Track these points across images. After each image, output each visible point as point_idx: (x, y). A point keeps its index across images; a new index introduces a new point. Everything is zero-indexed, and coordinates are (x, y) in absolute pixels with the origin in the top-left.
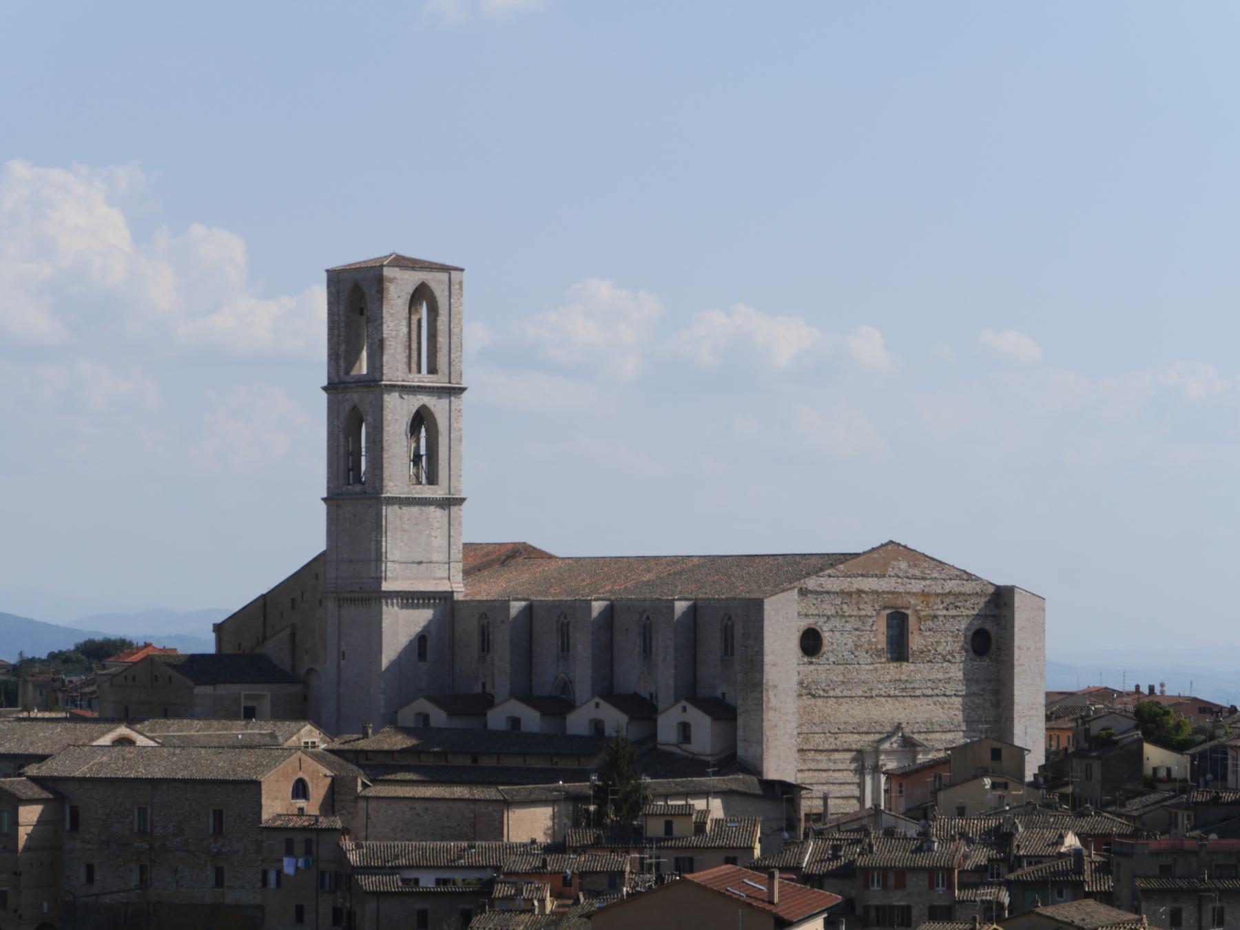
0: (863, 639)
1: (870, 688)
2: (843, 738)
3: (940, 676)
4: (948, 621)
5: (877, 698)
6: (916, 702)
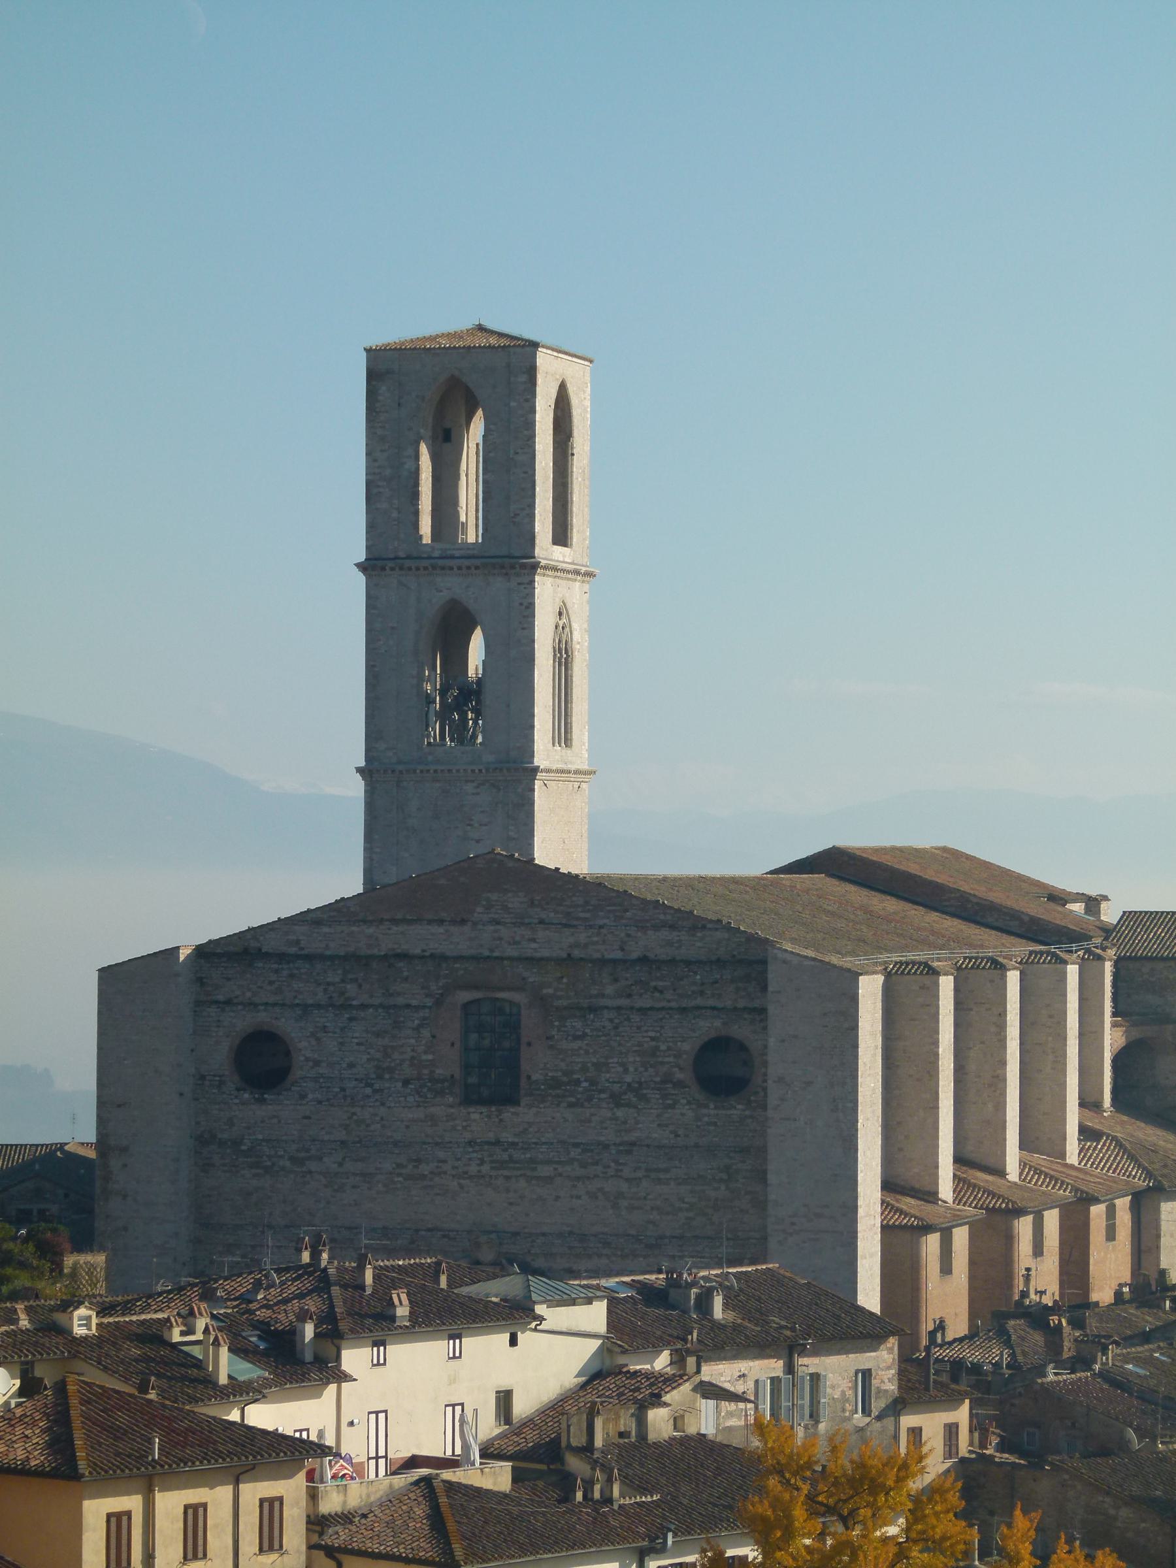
0: (396, 1056)
5: (437, 1179)
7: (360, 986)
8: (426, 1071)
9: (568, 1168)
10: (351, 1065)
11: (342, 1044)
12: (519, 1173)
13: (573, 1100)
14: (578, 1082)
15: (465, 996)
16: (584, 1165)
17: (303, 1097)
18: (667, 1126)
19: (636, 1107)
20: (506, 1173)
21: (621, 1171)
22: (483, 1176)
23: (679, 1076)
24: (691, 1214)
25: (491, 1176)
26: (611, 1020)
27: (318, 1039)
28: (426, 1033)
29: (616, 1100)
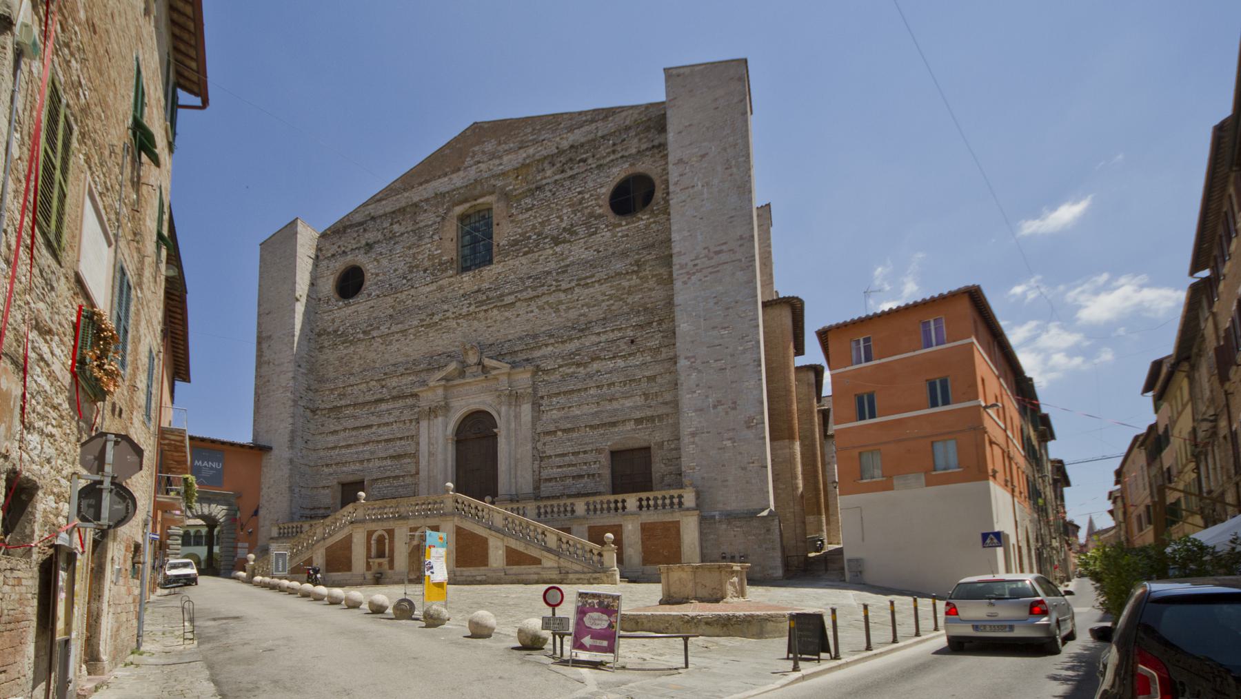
0: (420, 257)
1: (430, 312)
2: (393, 382)
3: (552, 265)
4: (563, 186)
5: (444, 323)
6: (506, 314)
8: (437, 261)
9: (525, 293)
10: (395, 270)
11: (391, 260)
12: (492, 306)
13: (527, 249)
14: (530, 237)
15: (459, 210)
16: (534, 288)
17: (369, 295)
18: (591, 247)
19: (569, 241)
20: (484, 308)
21: (560, 285)
22: (471, 314)
23: (599, 211)
24: (612, 302)
25: (476, 313)
27: (378, 261)
28: (436, 237)
29: (556, 241)
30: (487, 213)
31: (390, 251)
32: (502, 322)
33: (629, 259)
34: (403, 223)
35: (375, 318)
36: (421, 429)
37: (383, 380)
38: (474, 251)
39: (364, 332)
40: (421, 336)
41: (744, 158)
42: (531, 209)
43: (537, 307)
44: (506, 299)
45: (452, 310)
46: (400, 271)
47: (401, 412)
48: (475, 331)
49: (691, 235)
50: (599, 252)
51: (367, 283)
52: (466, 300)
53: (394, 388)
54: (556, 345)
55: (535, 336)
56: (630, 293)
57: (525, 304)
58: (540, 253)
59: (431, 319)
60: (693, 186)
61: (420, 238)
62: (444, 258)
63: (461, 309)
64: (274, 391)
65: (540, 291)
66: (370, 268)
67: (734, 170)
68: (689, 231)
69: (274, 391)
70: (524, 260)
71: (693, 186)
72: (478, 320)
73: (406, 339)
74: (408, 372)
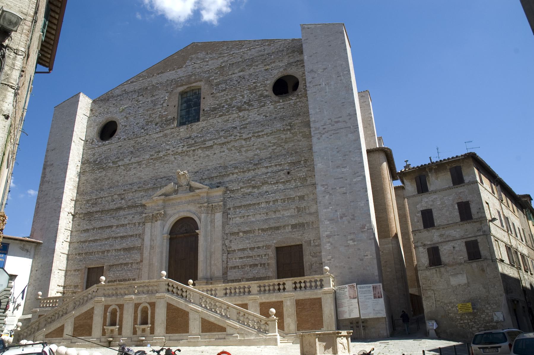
1: (157, 150)
3: (237, 123)
5: (166, 158)
6: (207, 153)
7: (143, 96)
8: (164, 118)
9: (219, 140)
10: (137, 124)
12: (198, 147)
13: (221, 113)
14: (223, 107)
16: (225, 138)
18: (262, 114)
19: (248, 110)
20: (193, 148)
22: (184, 152)
23: (266, 93)
24: (275, 147)
25: (187, 151)
26: (237, 81)
29: (240, 109)
30: (197, 91)
31: (135, 112)
32: (204, 158)
33: (285, 121)
34: (145, 96)
35: (121, 153)
36: (146, 229)
37: (123, 194)
38: (188, 113)
39: (113, 163)
40: (150, 165)
41: (347, 72)
42: (225, 90)
43: (227, 149)
44: (207, 143)
45: (172, 149)
46: (141, 124)
47: (133, 217)
48: (186, 163)
49: (320, 111)
50: (266, 117)
51: (118, 131)
52: (181, 143)
53: (130, 200)
54: (239, 174)
55: (225, 167)
56: (286, 142)
57: (219, 147)
58: (229, 116)
59: (158, 154)
60: (320, 85)
61: (155, 105)
62: (169, 117)
63: (177, 149)
64: (49, 201)
65: (229, 139)
66: (121, 122)
67: (342, 78)
68: (319, 109)
69: (49, 201)
70: (220, 120)
71: (320, 85)
72: (188, 156)
73: (140, 167)
74: (140, 189)
